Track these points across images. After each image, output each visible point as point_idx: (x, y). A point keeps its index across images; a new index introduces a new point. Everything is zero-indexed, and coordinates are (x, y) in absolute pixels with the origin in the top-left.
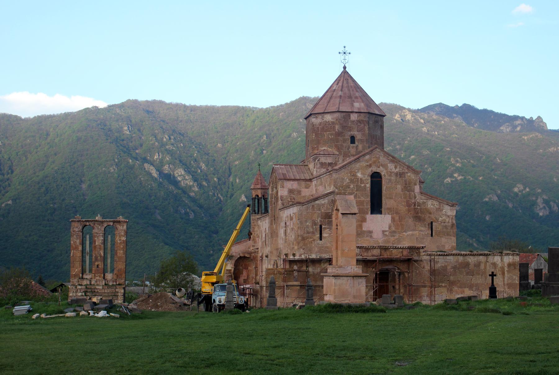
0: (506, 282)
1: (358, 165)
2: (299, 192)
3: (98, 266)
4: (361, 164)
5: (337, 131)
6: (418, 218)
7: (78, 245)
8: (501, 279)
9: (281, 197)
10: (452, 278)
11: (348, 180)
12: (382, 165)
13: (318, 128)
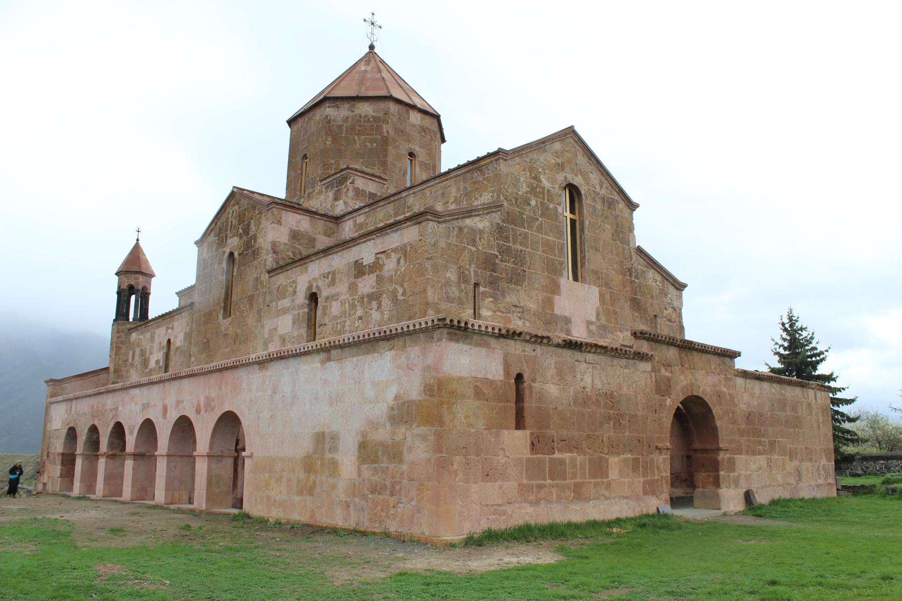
1: (542, 158)
2: (312, 241)
4: (548, 159)
5: (386, 134)
9: (274, 244)
11: (524, 186)
12: (582, 173)
13: (340, 127)
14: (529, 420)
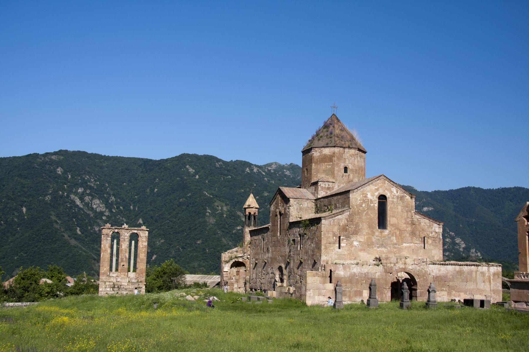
0: (492, 288)
1: (368, 189)
3: (123, 265)
6: (413, 234)
7: (107, 249)
8: (489, 286)
10: (451, 284)
14: (333, 280)
